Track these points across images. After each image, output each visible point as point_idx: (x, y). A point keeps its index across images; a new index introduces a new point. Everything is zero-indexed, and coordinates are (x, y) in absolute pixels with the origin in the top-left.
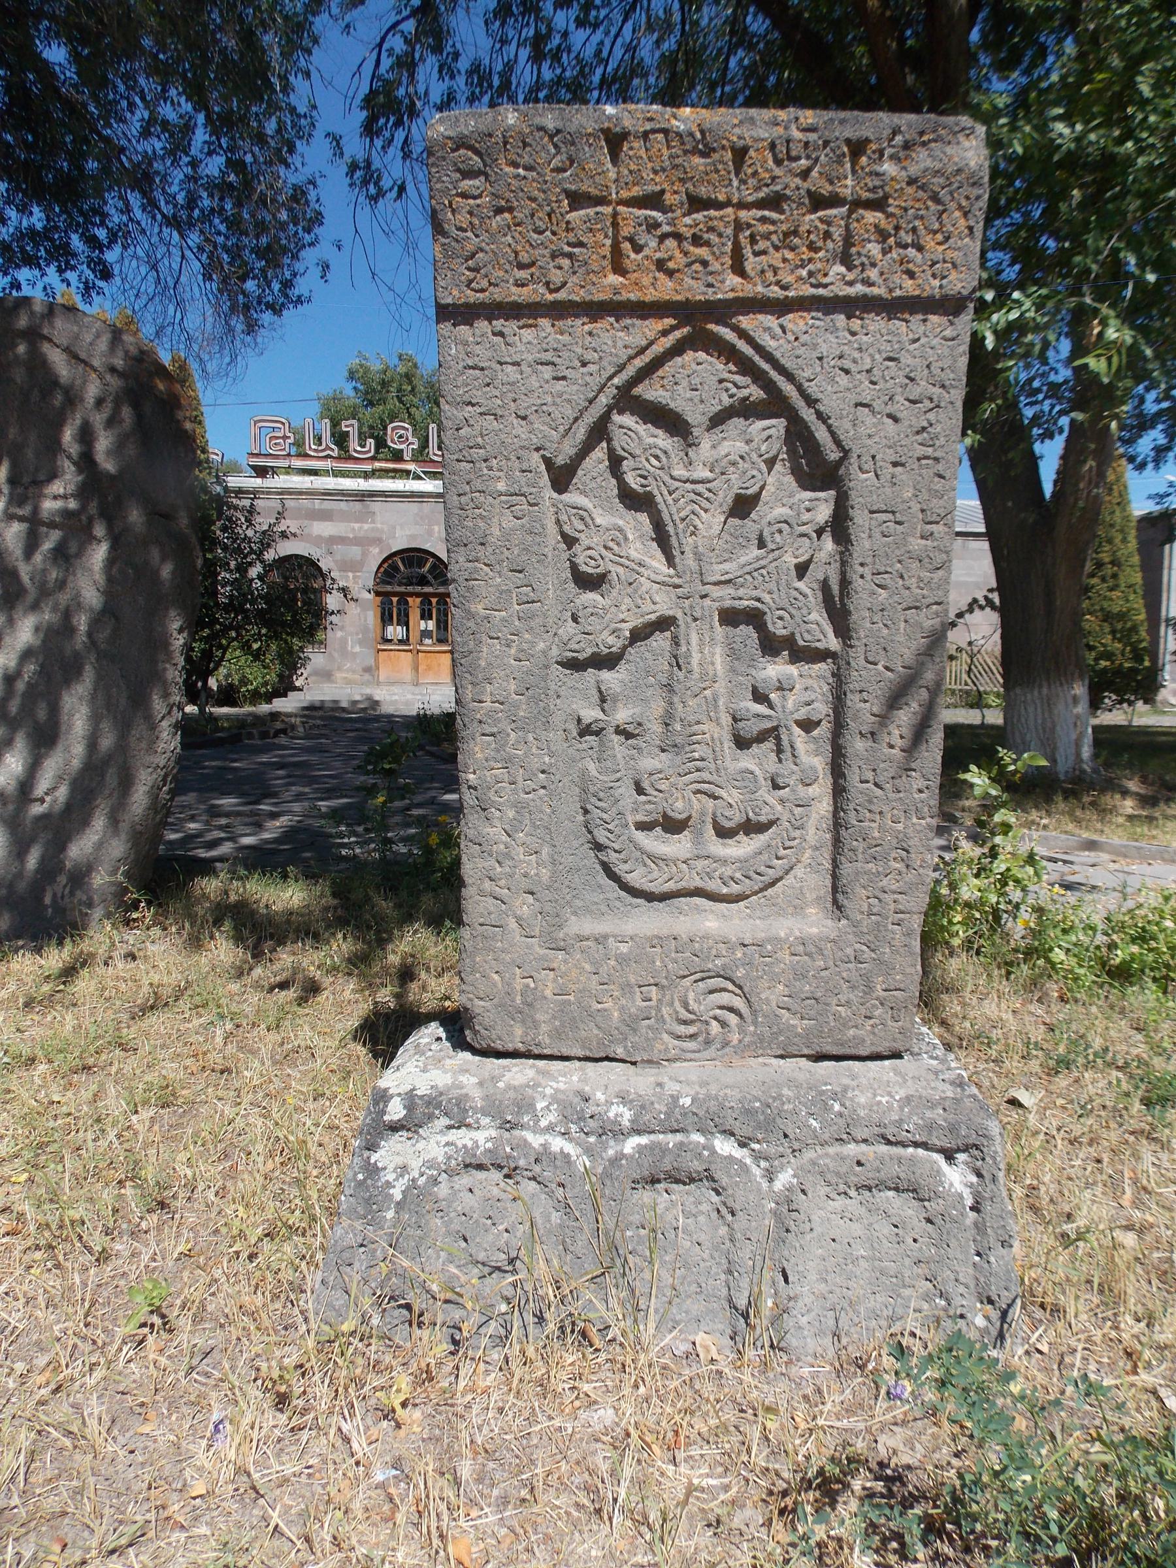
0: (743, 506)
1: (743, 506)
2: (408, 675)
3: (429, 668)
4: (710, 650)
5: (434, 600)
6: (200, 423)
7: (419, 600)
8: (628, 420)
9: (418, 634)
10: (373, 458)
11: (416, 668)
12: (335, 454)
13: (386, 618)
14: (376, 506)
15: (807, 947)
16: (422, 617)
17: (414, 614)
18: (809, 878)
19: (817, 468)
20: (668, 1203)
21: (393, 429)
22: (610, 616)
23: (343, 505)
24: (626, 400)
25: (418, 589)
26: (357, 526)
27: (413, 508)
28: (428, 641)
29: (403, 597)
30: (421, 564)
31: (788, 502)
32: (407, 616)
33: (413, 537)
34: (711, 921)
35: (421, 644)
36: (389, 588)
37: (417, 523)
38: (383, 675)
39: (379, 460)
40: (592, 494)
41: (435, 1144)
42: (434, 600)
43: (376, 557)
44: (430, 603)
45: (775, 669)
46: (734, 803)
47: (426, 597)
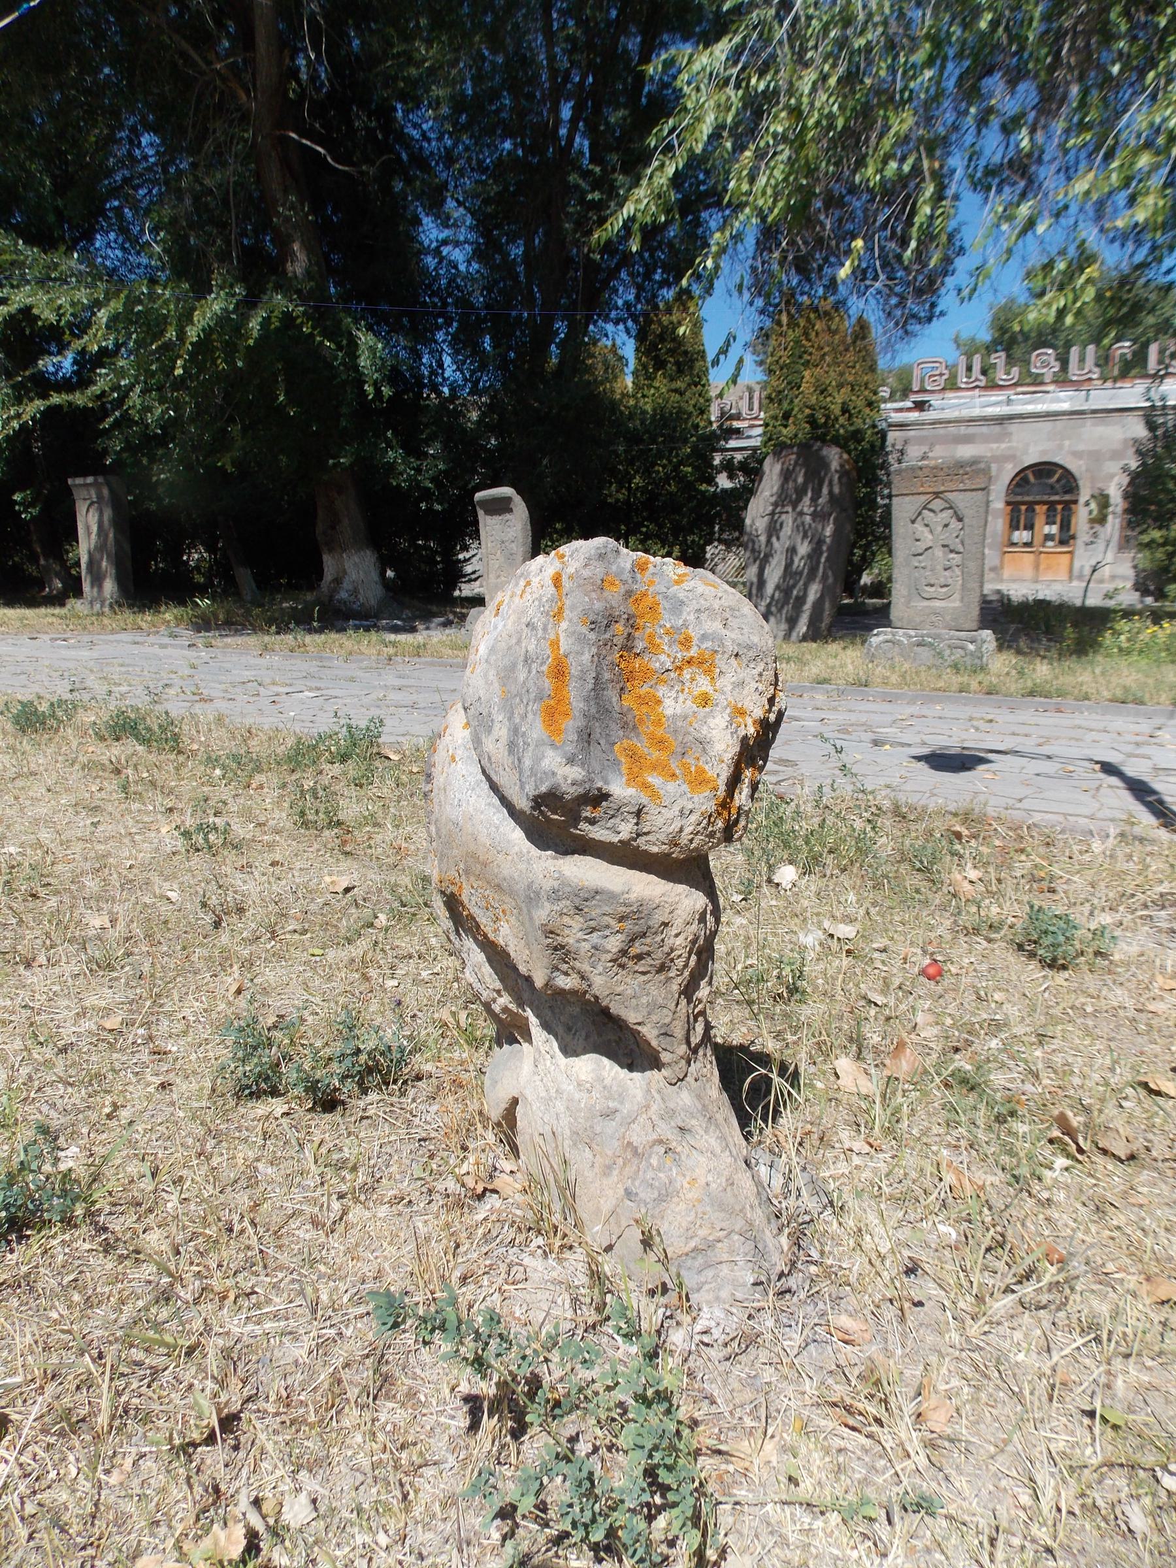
0: (946, 526)
1: (946, 526)
2: (1029, 573)
3: (1048, 568)
4: (939, 552)
8: (925, 512)
11: (1037, 567)
12: (982, 384)
13: (1014, 525)
14: (1013, 428)
15: (955, 608)
17: (1040, 520)
18: (957, 596)
19: (960, 520)
20: (920, 649)
22: (921, 546)
23: (984, 429)
24: (925, 508)
26: (995, 446)
27: (1046, 426)
28: (1050, 544)
29: (1031, 506)
30: (1050, 474)
31: (955, 524)
33: (1044, 452)
34: (937, 604)
36: (1019, 498)
38: (1006, 573)
40: (919, 526)
41: (881, 638)
42: (1059, 507)
43: (1009, 471)
45: (952, 555)
46: (942, 581)
47: (1052, 505)
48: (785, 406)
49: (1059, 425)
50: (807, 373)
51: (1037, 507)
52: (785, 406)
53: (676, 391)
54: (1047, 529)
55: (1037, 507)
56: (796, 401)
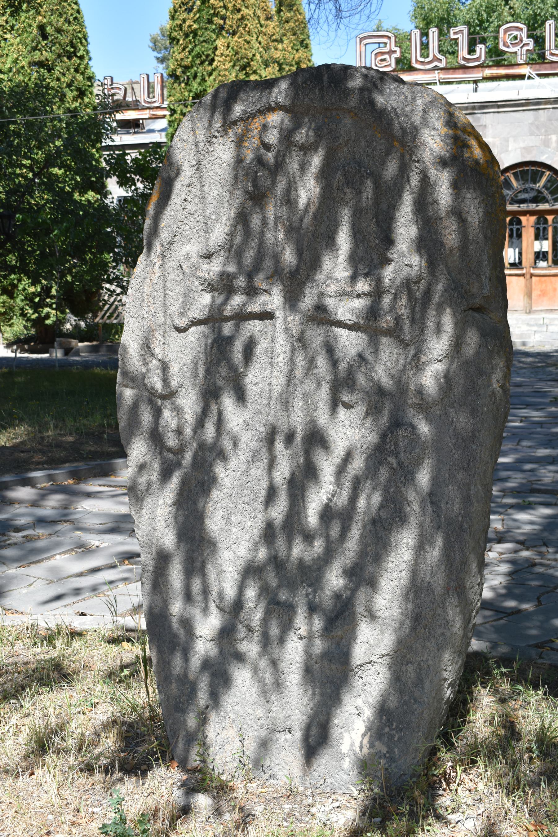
3: (544, 293)
5: (550, 218)
6: (307, 46)
7: (533, 219)
9: (532, 257)
10: (482, 66)
11: (529, 294)
16: (537, 238)
17: (528, 233)
21: (506, 31)
25: (533, 206)
27: (526, 117)
28: (542, 264)
32: (519, 236)
33: (527, 149)
35: (535, 267)
37: (532, 134)
39: (489, 67)
44: (546, 221)
47: (541, 215)
48: (195, 86)
49: (543, 115)
50: (220, 43)
51: (523, 219)
52: (195, 86)
53: (41, 64)
54: (537, 246)
55: (523, 219)
56: (210, 80)
